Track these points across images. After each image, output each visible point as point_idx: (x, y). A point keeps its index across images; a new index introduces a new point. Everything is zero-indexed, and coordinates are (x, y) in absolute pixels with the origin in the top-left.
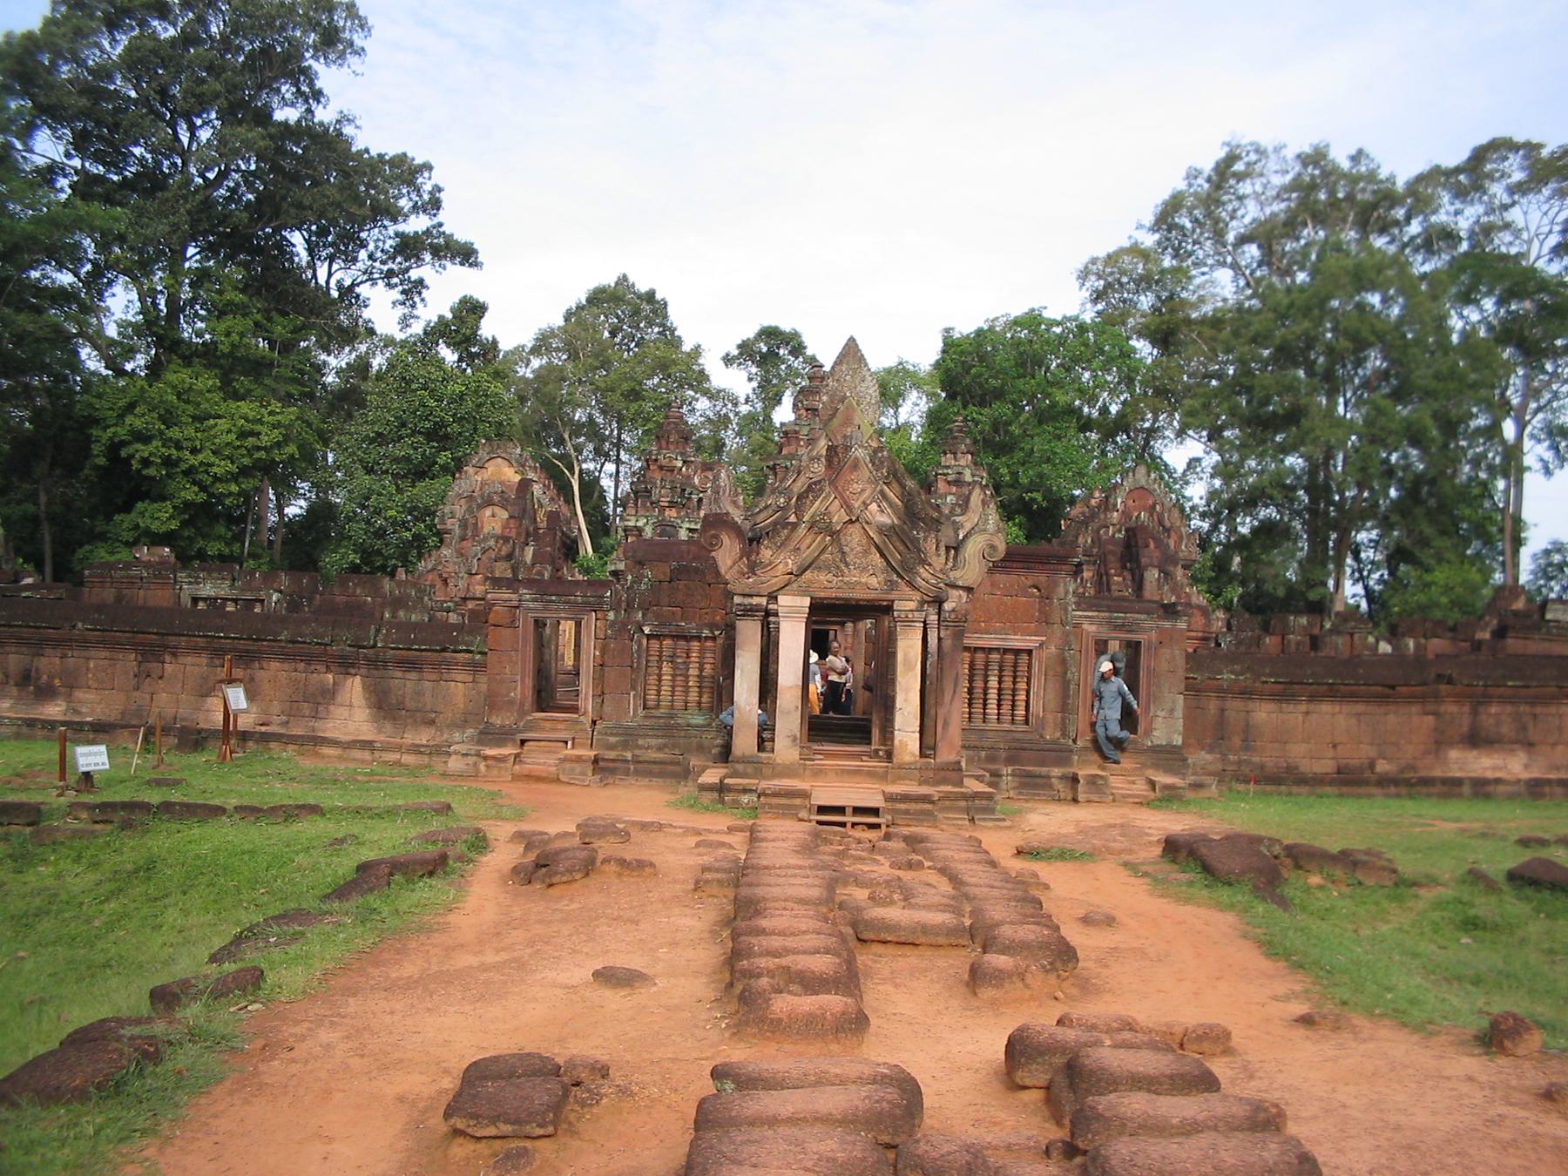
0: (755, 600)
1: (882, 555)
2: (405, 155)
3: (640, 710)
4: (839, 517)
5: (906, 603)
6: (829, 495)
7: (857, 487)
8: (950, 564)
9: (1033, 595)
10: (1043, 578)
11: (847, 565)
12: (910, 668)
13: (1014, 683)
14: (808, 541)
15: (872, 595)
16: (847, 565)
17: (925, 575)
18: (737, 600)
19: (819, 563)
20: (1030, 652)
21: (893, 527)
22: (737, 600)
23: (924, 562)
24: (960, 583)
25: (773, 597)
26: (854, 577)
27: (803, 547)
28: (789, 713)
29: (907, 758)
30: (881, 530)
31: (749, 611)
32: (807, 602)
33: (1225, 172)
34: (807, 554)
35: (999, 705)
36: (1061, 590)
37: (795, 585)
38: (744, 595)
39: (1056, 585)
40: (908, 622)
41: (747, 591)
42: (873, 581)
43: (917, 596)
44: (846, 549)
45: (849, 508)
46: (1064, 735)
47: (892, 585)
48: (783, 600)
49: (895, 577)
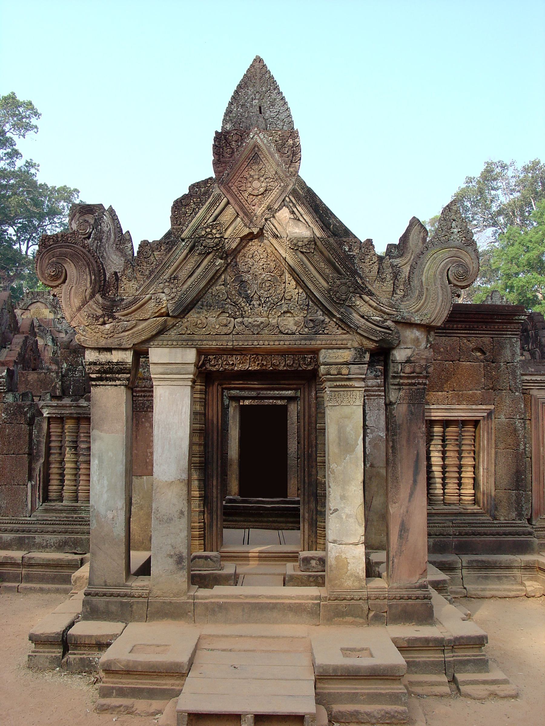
0: (116, 357)
1: (300, 283)
2: (65, 186)
3: (38, 503)
4: (234, 229)
5: (338, 353)
6: (218, 198)
7: (258, 186)
8: (400, 293)
9: (477, 359)
10: (487, 340)
11: (249, 299)
12: (346, 447)
13: (460, 458)
14: (189, 266)
15: (286, 343)
16: (249, 299)
17: (365, 309)
18: (90, 356)
19: (208, 297)
20: (476, 423)
21: (313, 241)
22: (90, 356)
23: (361, 290)
24: (416, 319)
25: (140, 353)
26: (258, 316)
27: (183, 274)
28: (170, 520)
29: (349, 583)
30: (296, 246)
31: (108, 373)
32: (191, 355)
33: (489, 175)
34: (190, 286)
35: (444, 485)
36: (507, 353)
37: (173, 333)
38: (101, 350)
39: (502, 347)
40: (343, 381)
41: (103, 343)
42: (289, 323)
43: (354, 341)
44: (247, 277)
45: (248, 215)
46: (520, 515)
47: (316, 328)
48: (157, 355)
49: (320, 316)
